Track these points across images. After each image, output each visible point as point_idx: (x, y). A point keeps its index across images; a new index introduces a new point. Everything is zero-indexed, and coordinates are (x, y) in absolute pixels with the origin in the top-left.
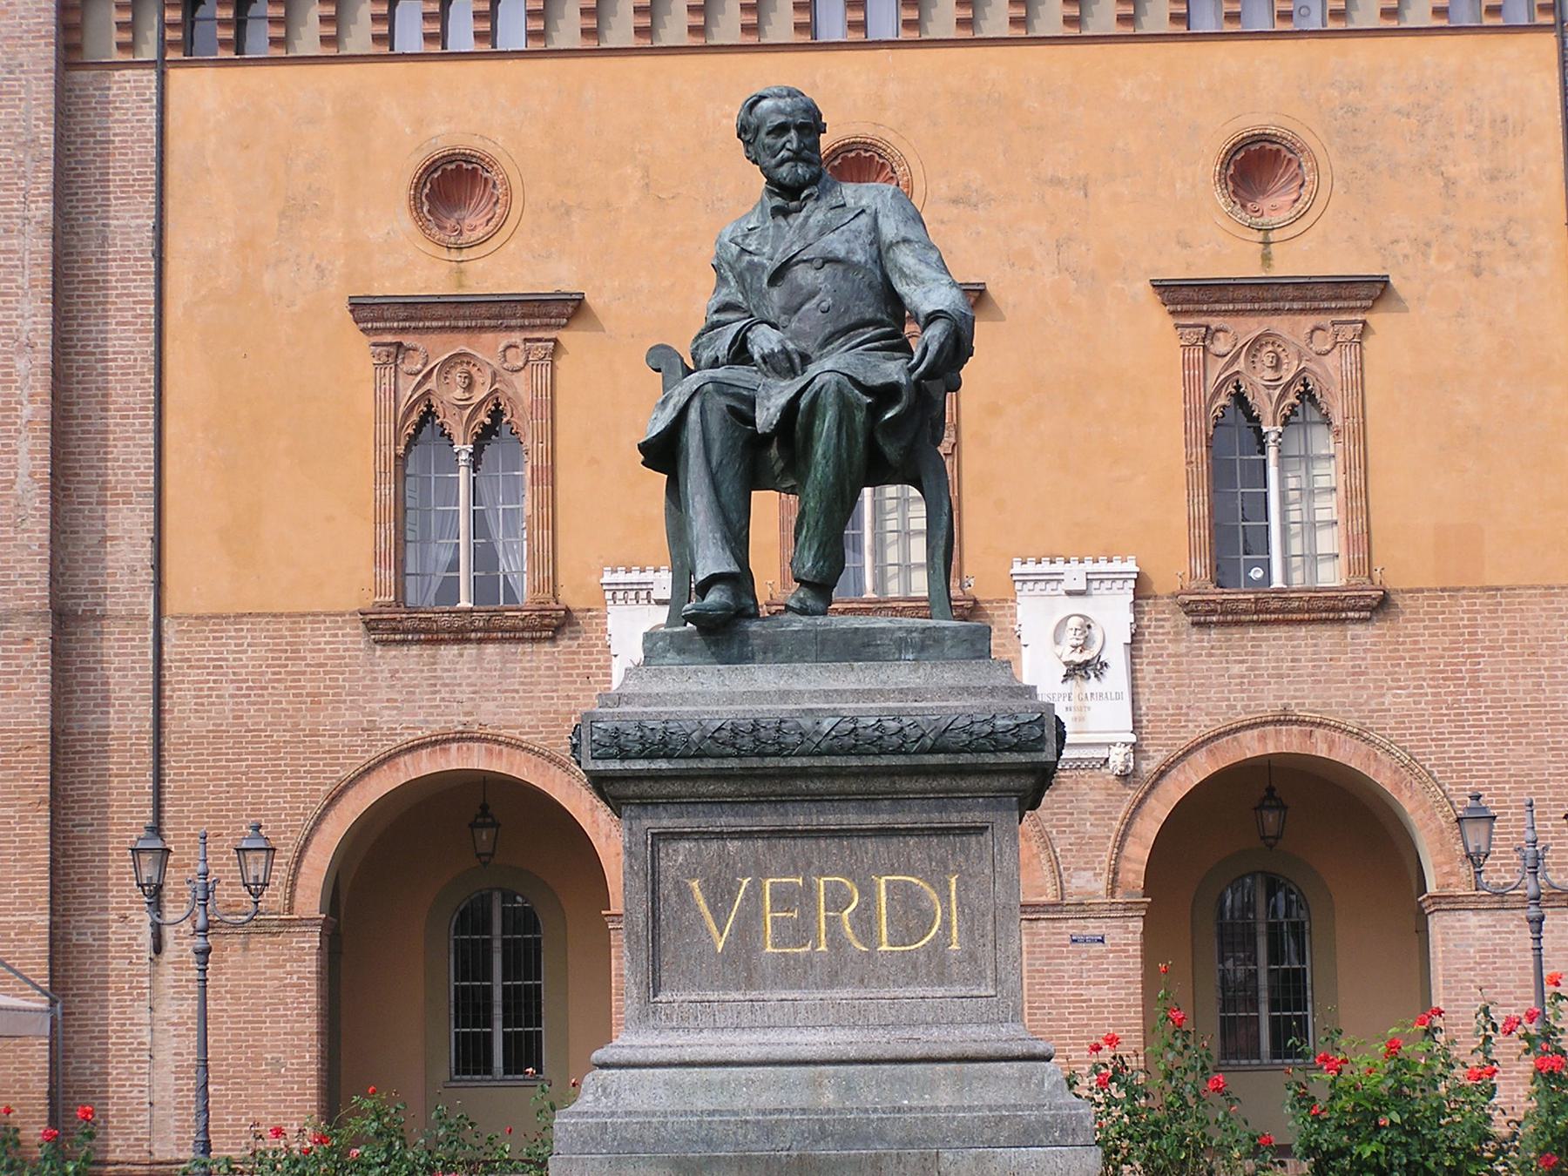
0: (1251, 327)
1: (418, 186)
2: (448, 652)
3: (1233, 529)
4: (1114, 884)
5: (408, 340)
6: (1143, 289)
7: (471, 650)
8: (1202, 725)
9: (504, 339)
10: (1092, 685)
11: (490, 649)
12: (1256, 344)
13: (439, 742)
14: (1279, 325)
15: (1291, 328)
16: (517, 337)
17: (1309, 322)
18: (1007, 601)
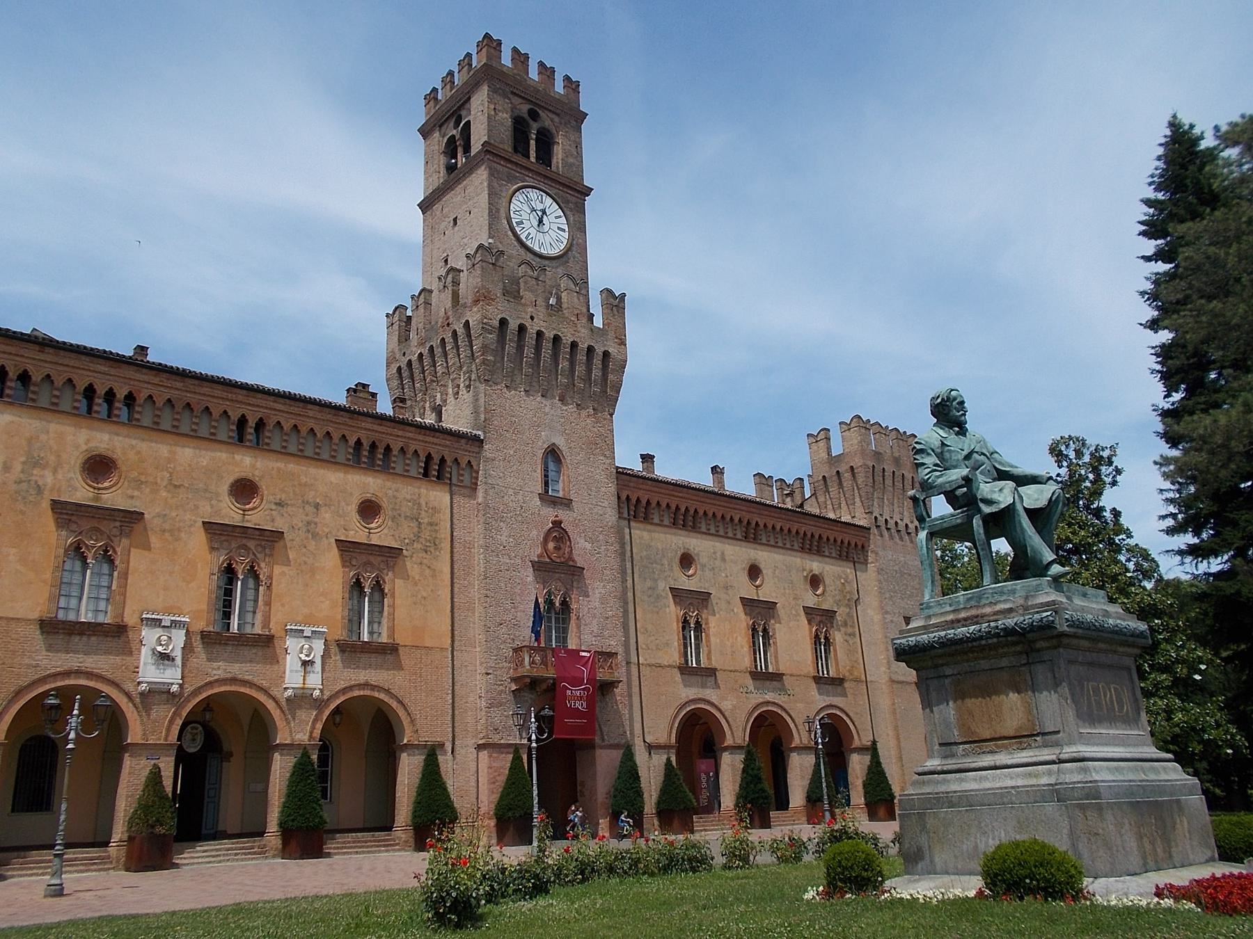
0: (364, 558)
1: (85, 463)
2: (76, 639)
3: (354, 620)
4: (311, 737)
5: (74, 518)
6: (333, 541)
7: (85, 638)
8: (343, 684)
9: (112, 524)
10: (309, 668)
11: (93, 638)
12: (365, 564)
13: (67, 674)
14: (372, 559)
15: (376, 560)
16: (118, 524)
17: (380, 559)
18: (283, 640)
